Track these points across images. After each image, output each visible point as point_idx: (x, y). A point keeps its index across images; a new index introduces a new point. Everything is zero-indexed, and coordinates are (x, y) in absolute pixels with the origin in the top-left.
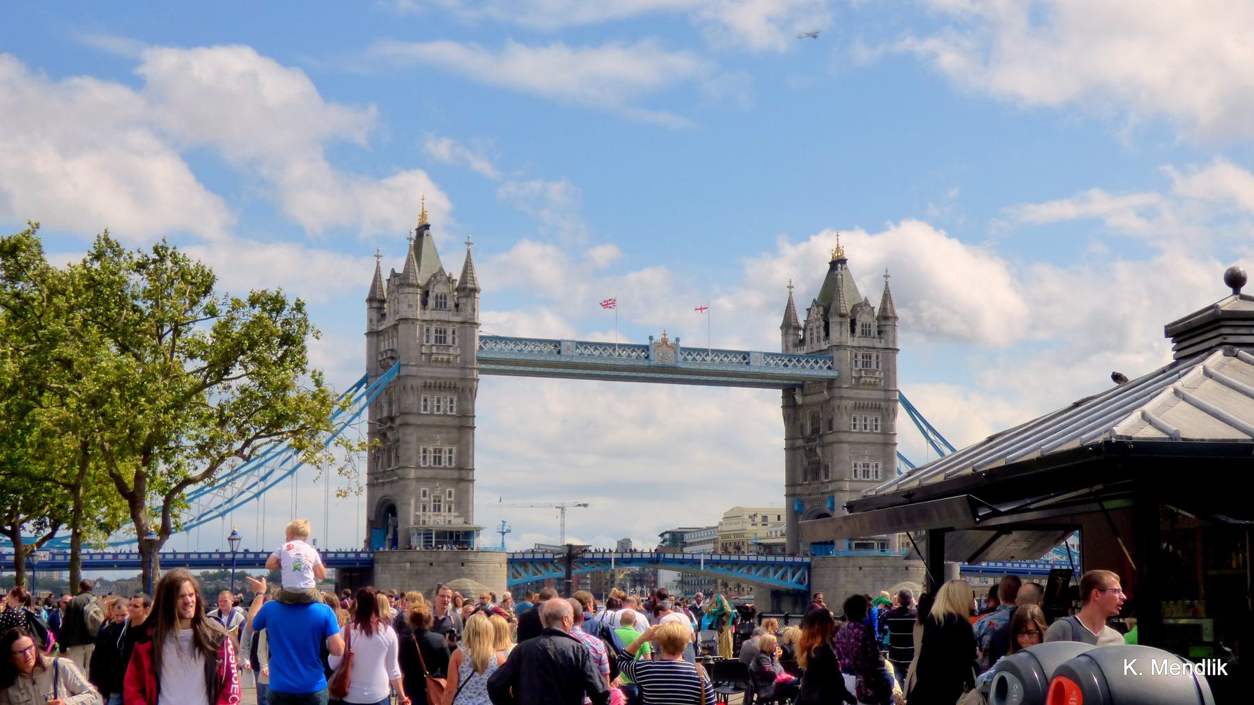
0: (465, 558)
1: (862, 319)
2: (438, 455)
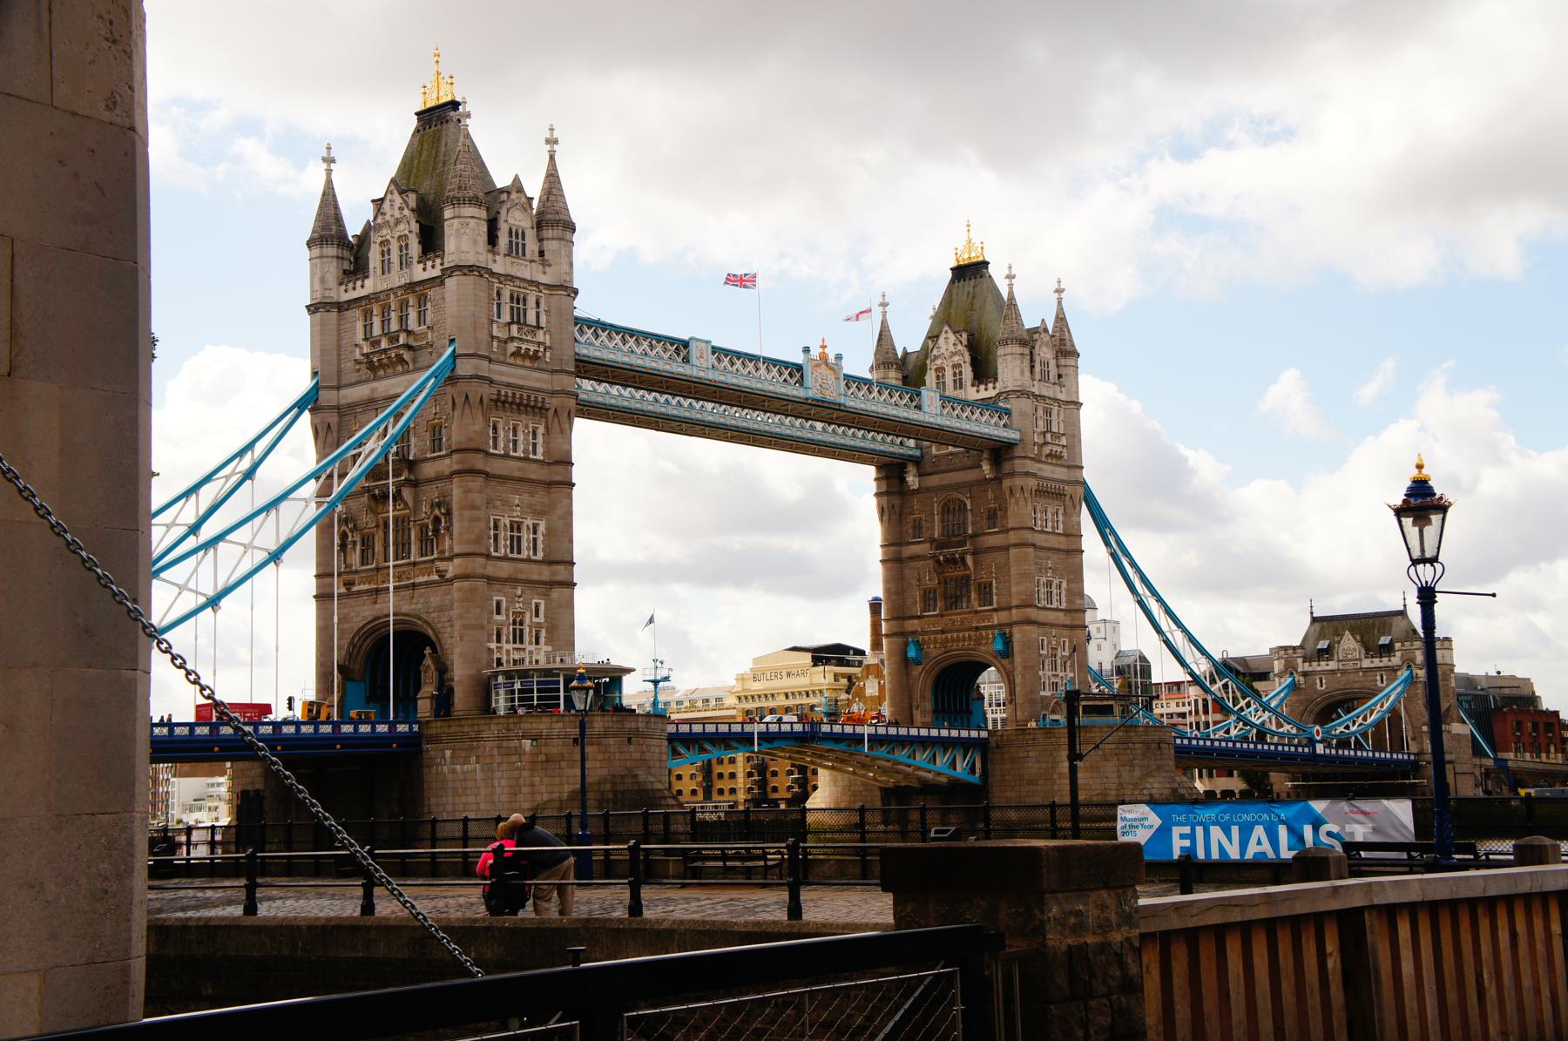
0: (633, 725)
1: (1045, 353)
2: (515, 534)
